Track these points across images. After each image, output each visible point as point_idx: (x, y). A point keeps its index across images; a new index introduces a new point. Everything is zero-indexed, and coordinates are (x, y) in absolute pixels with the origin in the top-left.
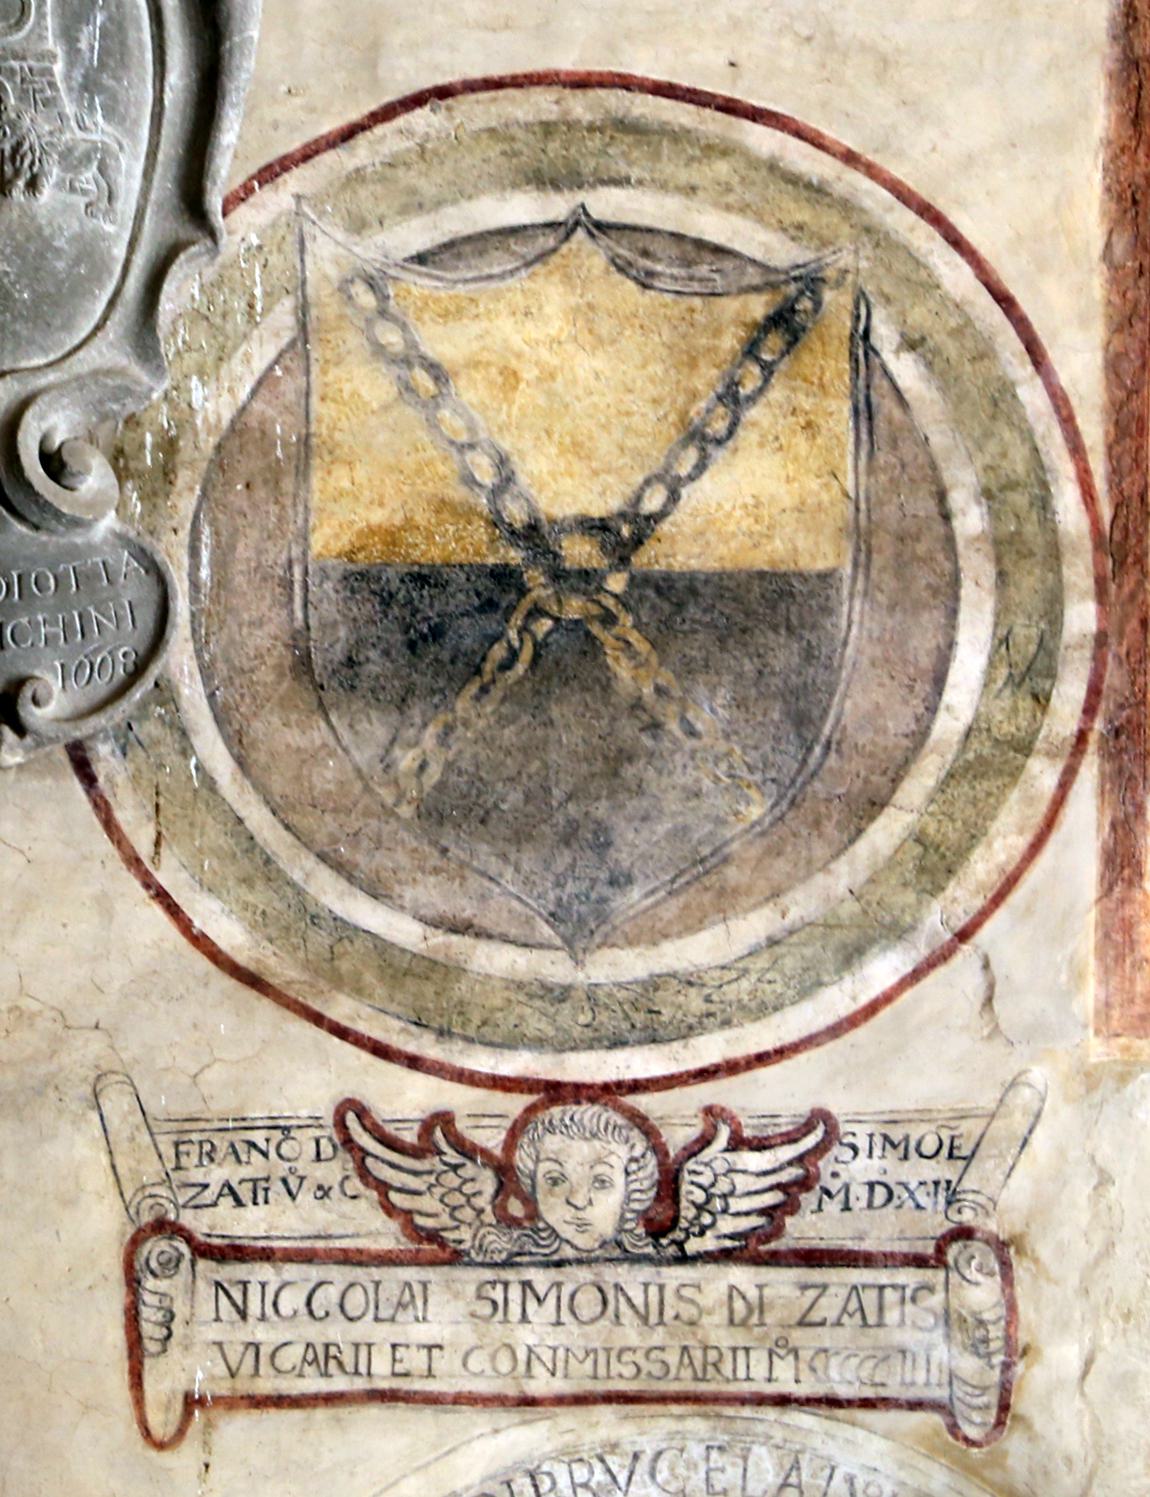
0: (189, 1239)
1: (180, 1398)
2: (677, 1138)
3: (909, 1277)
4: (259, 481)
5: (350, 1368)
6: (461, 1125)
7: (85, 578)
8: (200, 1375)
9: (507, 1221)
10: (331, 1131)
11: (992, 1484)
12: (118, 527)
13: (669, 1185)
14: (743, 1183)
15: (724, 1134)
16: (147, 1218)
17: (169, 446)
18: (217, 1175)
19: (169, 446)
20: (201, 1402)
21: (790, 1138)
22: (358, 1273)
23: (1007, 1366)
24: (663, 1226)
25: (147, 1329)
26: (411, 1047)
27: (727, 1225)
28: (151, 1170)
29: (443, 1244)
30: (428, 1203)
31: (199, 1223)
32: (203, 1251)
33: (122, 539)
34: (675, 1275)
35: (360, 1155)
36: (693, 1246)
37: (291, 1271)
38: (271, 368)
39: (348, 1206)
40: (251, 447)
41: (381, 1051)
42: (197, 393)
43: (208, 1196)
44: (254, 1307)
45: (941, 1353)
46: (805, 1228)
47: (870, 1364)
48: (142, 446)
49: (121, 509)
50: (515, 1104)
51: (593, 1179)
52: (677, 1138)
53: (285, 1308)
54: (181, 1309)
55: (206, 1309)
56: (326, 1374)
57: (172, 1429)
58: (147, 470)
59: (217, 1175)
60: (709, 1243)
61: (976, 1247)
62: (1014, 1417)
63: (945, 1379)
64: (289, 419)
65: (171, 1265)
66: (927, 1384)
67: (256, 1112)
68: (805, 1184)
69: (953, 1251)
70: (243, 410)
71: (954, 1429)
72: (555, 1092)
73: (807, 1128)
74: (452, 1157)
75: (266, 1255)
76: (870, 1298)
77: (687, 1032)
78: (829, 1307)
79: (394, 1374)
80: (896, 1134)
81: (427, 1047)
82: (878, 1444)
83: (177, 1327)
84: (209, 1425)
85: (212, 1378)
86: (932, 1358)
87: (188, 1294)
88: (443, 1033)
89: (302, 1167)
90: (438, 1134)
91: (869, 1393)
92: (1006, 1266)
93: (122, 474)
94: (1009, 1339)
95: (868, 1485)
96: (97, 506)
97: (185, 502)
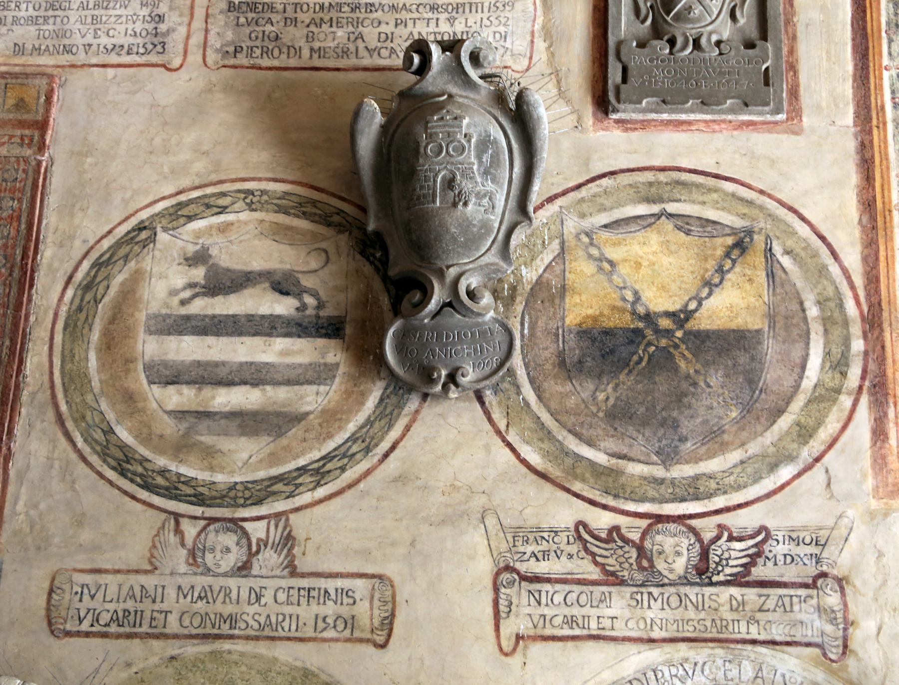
0: (518, 573)
1: (514, 636)
2: (707, 536)
3: (802, 592)
4: (546, 300)
5: (581, 626)
6: (623, 531)
7: (482, 333)
8: (522, 627)
9: (641, 568)
10: (573, 533)
11: (843, 679)
12: (494, 316)
13: (705, 554)
14: (734, 554)
15: (726, 535)
16: (502, 565)
17: (513, 289)
18: (529, 549)
19: (513, 289)
20: (523, 638)
21: (752, 537)
22: (584, 588)
23: (845, 629)
24: (703, 571)
25: (502, 608)
26: (604, 501)
27: (728, 571)
28: (504, 547)
29: (617, 577)
30: (611, 561)
31: (522, 567)
32: (524, 578)
33: (496, 320)
34: (708, 590)
35: (584, 542)
36: (715, 579)
37: (558, 587)
38: (551, 263)
39: (580, 562)
40: (543, 289)
41: (592, 503)
42: (524, 270)
43: (526, 557)
44: (543, 601)
45: (817, 623)
46: (760, 572)
47: (788, 627)
48: (504, 289)
49: (496, 310)
50: (644, 523)
51: (675, 553)
52: (707, 536)
53: (556, 602)
54: (515, 601)
55: (525, 601)
56: (572, 628)
57: (511, 648)
58: (505, 296)
59: (529, 549)
60: (721, 578)
61: (829, 580)
62: (850, 651)
63: (820, 634)
64: (558, 279)
65: (511, 583)
66: (812, 636)
67: (544, 525)
68: (759, 554)
69: (820, 582)
70: (541, 276)
71: (825, 655)
72: (660, 519)
73: (758, 533)
74: (620, 543)
75: (548, 580)
76: (787, 600)
77: (710, 496)
78: (770, 604)
79: (599, 629)
80: (794, 535)
81: (610, 501)
82: (794, 661)
83: (513, 607)
84: (526, 647)
85: (527, 628)
86: (814, 626)
87: (518, 596)
88: (616, 496)
89: (562, 546)
90: (615, 534)
91: (788, 639)
92: (842, 589)
93: (496, 299)
94: (845, 618)
95: (791, 678)
96: (487, 309)
97: (519, 308)
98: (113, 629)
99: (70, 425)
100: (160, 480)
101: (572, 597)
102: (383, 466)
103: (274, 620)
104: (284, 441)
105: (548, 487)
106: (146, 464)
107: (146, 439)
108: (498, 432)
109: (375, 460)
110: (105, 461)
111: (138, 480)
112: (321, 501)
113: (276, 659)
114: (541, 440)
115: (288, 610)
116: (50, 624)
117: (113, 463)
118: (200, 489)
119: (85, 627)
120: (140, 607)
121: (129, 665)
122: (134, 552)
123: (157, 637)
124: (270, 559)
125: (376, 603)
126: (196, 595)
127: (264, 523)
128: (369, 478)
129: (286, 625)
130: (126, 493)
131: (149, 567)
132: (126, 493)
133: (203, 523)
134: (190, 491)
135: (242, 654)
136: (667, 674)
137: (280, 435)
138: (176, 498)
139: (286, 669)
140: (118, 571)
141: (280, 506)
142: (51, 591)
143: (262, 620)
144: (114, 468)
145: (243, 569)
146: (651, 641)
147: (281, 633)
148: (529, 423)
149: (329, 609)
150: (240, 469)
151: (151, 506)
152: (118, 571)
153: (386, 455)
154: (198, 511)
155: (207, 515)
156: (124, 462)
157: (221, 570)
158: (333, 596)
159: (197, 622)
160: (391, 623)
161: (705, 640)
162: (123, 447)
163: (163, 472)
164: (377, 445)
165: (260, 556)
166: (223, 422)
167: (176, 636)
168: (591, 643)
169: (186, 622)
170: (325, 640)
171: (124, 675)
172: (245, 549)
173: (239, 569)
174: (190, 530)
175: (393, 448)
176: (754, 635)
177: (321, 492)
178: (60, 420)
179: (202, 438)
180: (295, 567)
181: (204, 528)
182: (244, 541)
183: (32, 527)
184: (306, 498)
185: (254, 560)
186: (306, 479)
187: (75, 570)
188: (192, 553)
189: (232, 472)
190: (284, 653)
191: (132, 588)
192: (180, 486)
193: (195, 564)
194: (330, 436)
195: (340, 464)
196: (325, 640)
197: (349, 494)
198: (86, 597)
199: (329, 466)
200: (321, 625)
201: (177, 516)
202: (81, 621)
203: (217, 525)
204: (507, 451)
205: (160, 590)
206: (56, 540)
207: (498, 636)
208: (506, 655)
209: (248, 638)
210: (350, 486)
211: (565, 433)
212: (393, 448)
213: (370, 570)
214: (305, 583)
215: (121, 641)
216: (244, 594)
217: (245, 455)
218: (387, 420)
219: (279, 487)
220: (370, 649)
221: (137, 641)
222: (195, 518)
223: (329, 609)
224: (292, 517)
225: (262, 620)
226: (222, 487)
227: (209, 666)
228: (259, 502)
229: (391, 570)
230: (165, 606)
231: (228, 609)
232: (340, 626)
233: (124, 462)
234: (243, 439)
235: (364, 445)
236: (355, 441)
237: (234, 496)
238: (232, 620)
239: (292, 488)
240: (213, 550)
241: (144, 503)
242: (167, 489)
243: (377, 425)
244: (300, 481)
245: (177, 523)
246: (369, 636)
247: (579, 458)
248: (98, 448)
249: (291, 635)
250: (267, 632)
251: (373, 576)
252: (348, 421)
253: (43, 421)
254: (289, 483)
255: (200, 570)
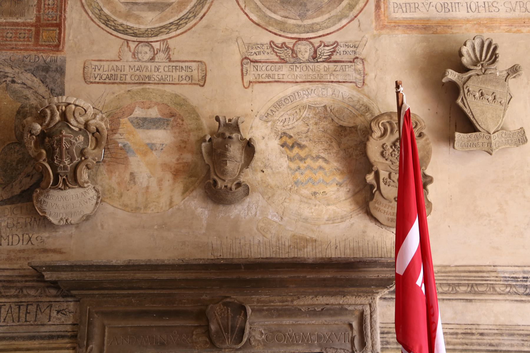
0: (250, 60)
2: (316, 45)
3: (349, 64)
6: (287, 44)
9: (293, 57)
13: (315, 52)
14: (326, 51)
15: (323, 45)
16: (244, 57)
18: (253, 51)
21: (332, 45)
23: (364, 77)
24: (315, 58)
25: (244, 72)
26: (280, 33)
27: (324, 57)
28: (244, 50)
30: (282, 55)
31: (251, 58)
32: (252, 61)
34: (317, 64)
35: (273, 48)
36: (319, 60)
37: (264, 64)
39: (272, 55)
41: (276, 34)
43: (252, 54)
44: (259, 69)
45: (354, 75)
46: (335, 57)
50: (294, 41)
51: (305, 51)
52: (316, 45)
55: (252, 69)
59: (253, 51)
60: (321, 60)
61: (359, 60)
65: (247, 63)
67: (259, 42)
68: (334, 51)
69: (355, 60)
71: (356, 86)
72: (299, 39)
73: (334, 44)
74: (286, 48)
75: (260, 62)
76: (344, 67)
77: (318, 31)
78: (338, 69)
80: (347, 44)
81: (282, 33)
82: (345, 88)
84: (253, 85)
86: (352, 75)
87: (250, 67)
88: (284, 32)
89: (265, 50)
91: (344, 81)
92: (363, 62)
94: (364, 73)
98: (107, 81)
99: (86, 7)
100: (120, 28)
101: (269, 68)
102: (200, 22)
103: (164, 77)
104: (164, 13)
105: (260, 28)
106: (115, 22)
107: (115, 13)
108: (242, 9)
109: (198, 20)
110: (100, 21)
111: (113, 27)
112: (179, 35)
113: (165, 91)
114: (257, 11)
115: (169, 74)
116: (85, 79)
117: (103, 22)
118: (135, 31)
119: (97, 80)
120: (116, 73)
121: (113, 93)
122: (113, 54)
123: (123, 83)
124: (161, 56)
125: (200, 71)
126: (136, 69)
127: (159, 43)
128: (196, 26)
129: (168, 79)
130: (108, 32)
131: (118, 59)
132: (108, 32)
133: (137, 43)
134: (132, 32)
135: (153, 89)
136: (302, 94)
137: (163, 11)
138: (127, 34)
139: (169, 94)
140: (108, 61)
141: (164, 37)
142: (84, 68)
143: (160, 77)
144: (103, 23)
145: (152, 59)
146: (297, 82)
147: (167, 82)
148: (253, 5)
149: (183, 73)
150: (149, 23)
151: (118, 37)
152: (108, 61)
153: (202, 18)
154: (135, 39)
155: (138, 40)
156: (107, 21)
157: (144, 60)
158: (184, 69)
159: (137, 78)
160: (205, 78)
161: (315, 82)
162: (106, 16)
163: (121, 25)
164: (198, 14)
165: (158, 55)
166: (142, 6)
167: (129, 83)
168: (276, 84)
169: (133, 78)
170: (182, 84)
171: (112, 97)
172: (152, 52)
173: (151, 59)
174: (133, 46)
175: (204, 15)
176: (333, 80)
177: (179, 32)
178: (83, 6)
179: (135, 12)
180: (170, 59)
181: (138, 45)
182: (152, 49)
183: (76, 45)
184: (173, 34)
185: (156, 56)
186: (173, 27)
187: (92, 60)
188: (134, 54)
189: (146, 25)
190: (168, 89)
191: (113, 66)
192: (128, 30)
193: (135, 58)
194: (181, 11)
195: (185, 21)
196: (182, 84)
197: (189, 32)
198: (97, 70)
199: (181, 22)
200: (180, 79)
201: (127, 41)
202: (96, 78)
203: (142, 44)
204: (245, 15)
205: (123, 67)
206: (85, 50)
207: (243, 82)
208: (246, 88)
209: (155, 84)
210: (189, 29)
211: (266, 9)
212: (204, 15)
213: (197, 59)
214: (174, 64)
215: (110, 85)
216: (153, 68)
217: (151, 19)
218: (201, 5)
219: (163, 30)
220: (198, 87)
221: (116, 85)
222: (134, 41)
223: (183, 73)
224: (169, 40)
225: (160, 77)
226: (143, 30)
227: (142, 93)
228: (157, 35)
229: (204, 59)
230: (125, 73)
231: (148, 74)
232: (188, 79)
233: (107, 21)
234: (150, 13)
235: (193, 14)
236: (190, 13)
237: (147, 33)
238: (149, 77)
239: (168, 30)
240: (141, 53)
241: (115, 36)
242: (123, 31)
243: (198, 7)
244: (171, 27)
245: (128, 43)
246: (197, 82)
247: (271, 18)
248: (97, 16)
249: (170, 82)
250: (162, 82)
251: (198, 62)
252: (187, 6)
253: (76, 6)
254: (167, 28)
255: (137, 60)
